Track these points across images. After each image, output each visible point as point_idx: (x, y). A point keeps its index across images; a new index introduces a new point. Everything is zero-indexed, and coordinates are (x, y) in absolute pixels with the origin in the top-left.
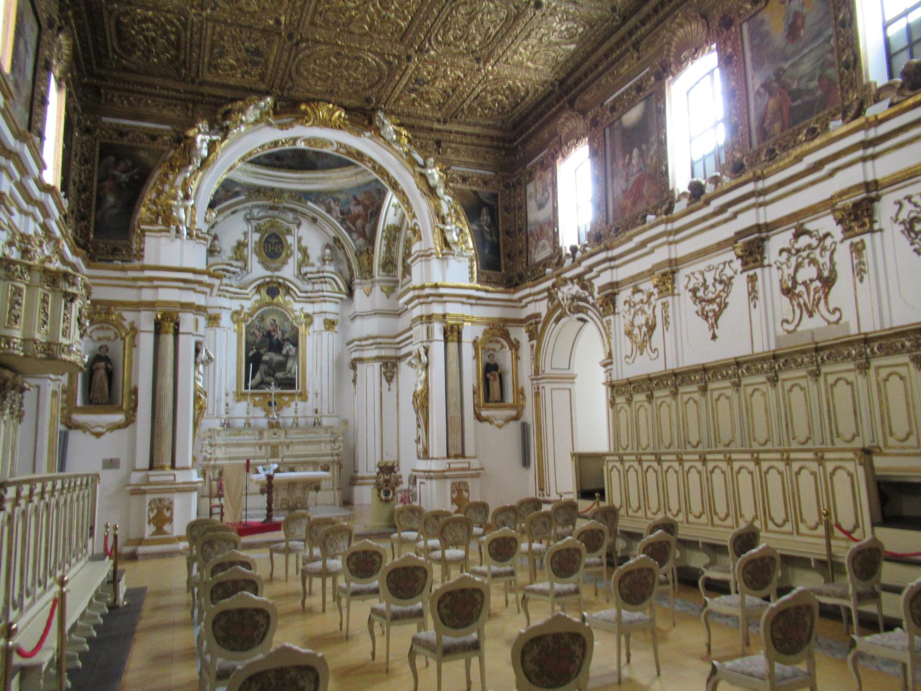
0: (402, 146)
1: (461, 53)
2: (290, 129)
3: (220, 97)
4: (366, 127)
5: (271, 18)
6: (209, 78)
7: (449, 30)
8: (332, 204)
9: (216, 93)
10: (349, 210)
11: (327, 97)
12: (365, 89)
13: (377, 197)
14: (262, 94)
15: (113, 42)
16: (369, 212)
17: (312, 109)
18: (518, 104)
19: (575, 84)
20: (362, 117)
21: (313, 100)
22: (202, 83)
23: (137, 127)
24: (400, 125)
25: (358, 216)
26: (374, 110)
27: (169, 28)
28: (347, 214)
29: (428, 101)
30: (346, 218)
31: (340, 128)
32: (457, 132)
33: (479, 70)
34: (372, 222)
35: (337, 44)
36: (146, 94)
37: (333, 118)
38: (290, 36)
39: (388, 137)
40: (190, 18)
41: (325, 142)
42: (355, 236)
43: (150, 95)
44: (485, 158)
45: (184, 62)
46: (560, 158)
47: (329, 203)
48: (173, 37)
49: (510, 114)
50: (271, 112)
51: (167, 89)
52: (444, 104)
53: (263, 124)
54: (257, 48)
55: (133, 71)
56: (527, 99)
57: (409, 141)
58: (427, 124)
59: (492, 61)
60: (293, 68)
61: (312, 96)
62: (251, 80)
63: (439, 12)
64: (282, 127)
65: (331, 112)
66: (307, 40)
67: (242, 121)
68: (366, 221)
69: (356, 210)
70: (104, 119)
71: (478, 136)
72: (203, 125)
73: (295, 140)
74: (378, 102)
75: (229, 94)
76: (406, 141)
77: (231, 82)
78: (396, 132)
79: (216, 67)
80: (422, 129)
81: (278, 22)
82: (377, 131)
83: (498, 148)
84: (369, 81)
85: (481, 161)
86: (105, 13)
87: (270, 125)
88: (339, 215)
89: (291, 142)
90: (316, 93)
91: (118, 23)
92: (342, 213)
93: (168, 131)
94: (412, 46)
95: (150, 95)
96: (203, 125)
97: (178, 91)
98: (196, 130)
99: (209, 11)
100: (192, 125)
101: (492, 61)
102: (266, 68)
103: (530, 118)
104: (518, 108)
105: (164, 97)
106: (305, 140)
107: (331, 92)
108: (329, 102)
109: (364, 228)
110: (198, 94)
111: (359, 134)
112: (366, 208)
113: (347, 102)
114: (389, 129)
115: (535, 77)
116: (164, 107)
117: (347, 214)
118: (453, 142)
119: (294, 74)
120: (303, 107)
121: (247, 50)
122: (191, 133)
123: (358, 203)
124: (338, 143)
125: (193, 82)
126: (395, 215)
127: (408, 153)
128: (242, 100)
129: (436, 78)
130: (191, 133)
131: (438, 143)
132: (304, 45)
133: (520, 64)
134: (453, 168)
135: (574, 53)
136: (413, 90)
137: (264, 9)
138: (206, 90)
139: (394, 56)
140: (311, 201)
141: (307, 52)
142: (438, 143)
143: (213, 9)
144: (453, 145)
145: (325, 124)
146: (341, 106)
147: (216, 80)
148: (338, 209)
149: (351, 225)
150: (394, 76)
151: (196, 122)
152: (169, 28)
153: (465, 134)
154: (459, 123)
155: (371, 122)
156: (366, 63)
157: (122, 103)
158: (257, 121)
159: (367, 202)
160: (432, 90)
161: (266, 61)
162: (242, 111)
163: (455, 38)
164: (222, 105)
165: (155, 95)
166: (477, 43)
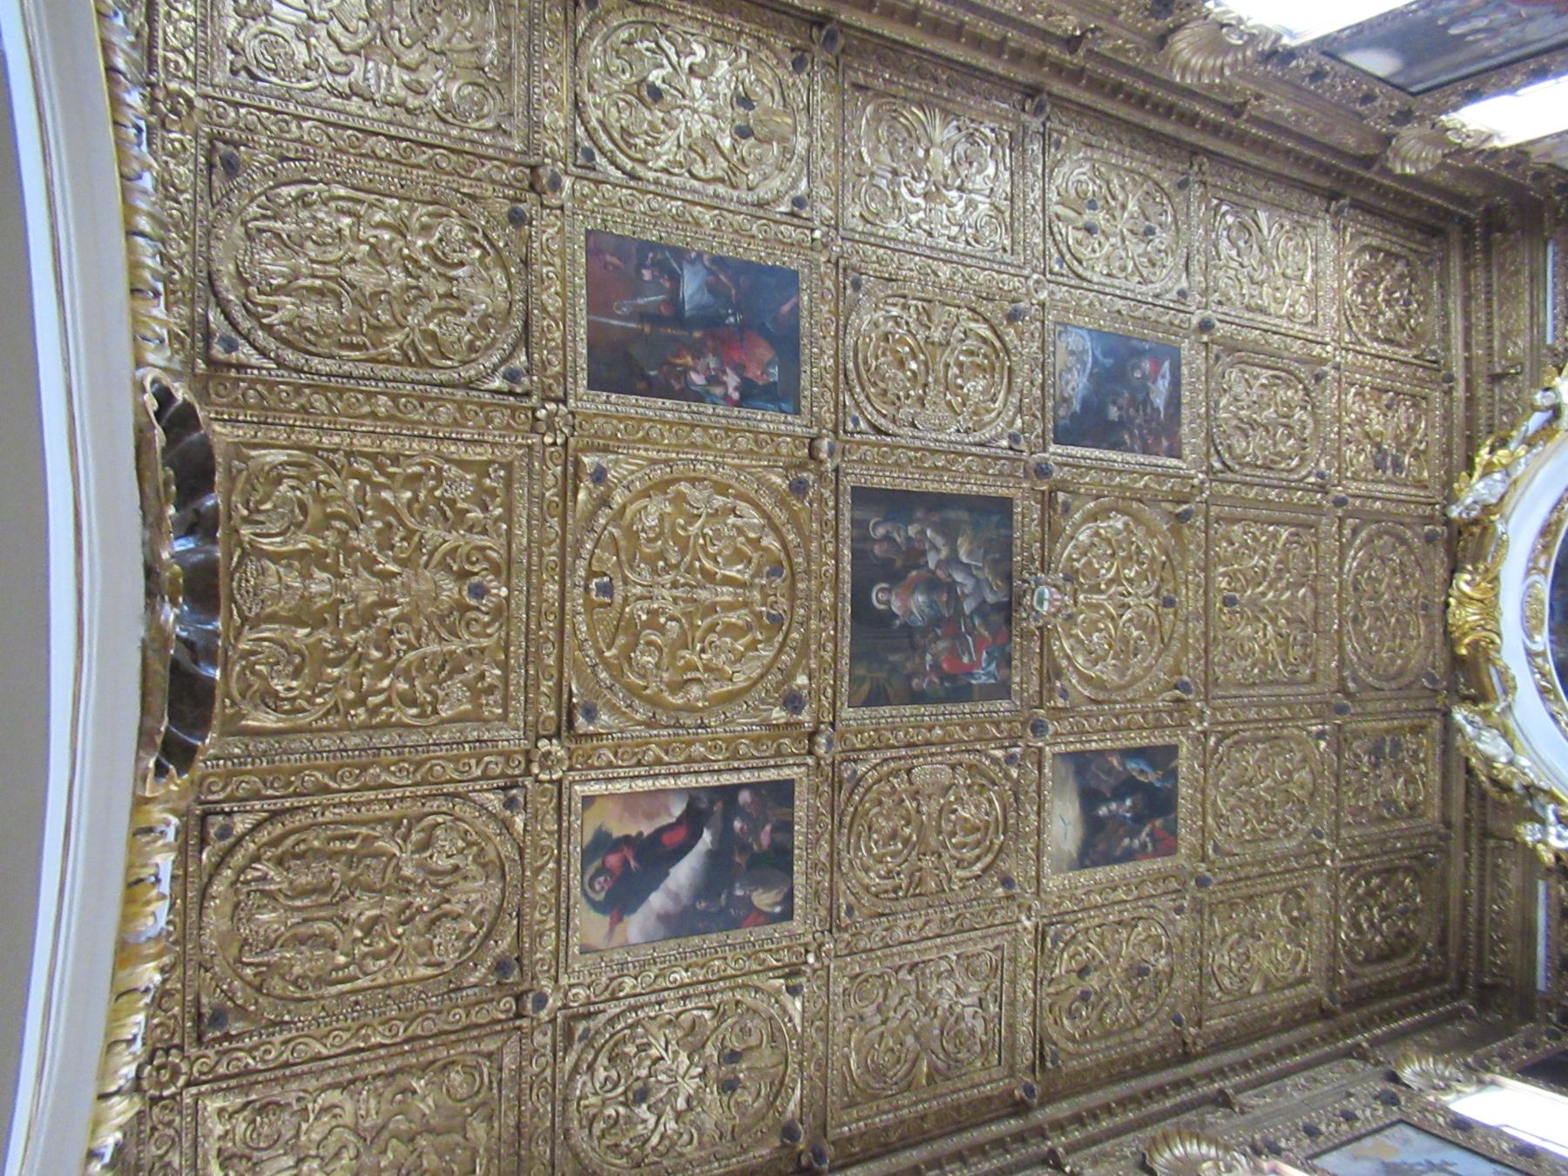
0: (1515, 459)
1: (1313, 414)
2: (1513, 672)
3: (1468, 791)
4: (1485, 529)
5: (1317, 746)
6: (1435, 813)
7: (1279, 454)
9: (1461, 800)
11: (1436, 612)
12: (1410, 550)
14: (1449, 728)
15: (1399, 967)
17: (1465, 635)
18: (1388, 254)
19: (1325, 170)
20: (1466, 542)
21: (1447, 633)
22: (1448, 824)
23: (1548, 937)
24: (1469, 465)
26: (1448, 522)
27: (1360, 891)
29: (1412, 429)
31: (1496, 578)
32: (1467, 346)
33: (1337, 367)
35: (1339, 632)
36: (1481, 910)
37: (1477, 595)
38: (1341, 710)
39: (1500, 489)
40: (1338, 864)
41: (1529, 598)
43: (1481, 904)
44: (1517, 272)
45: (1416, 857)
46: (1497, 143)
48: (1375, 881)
49: (1412, 257)
50: (1482, 706)
51: (1466, 877)
52: (1413, 396)
53: (1511, 723)
54: (1369, 753)
55: (1444, 931)
56: (1375, 242)
57: (1504, 443)
58: (1459, 411)
59: (1317, 350)
60: (1394, 685)
61: (1439, 638)
62: (1427, 745)
63: (1252, 485)
64: (1509, 688)
65: (1464, 600)
66: (1342, 679)
67: (1511, 763)
70: (1541, 984)
71: (1467, 300)
72: (1528, 833)
73: (1531, 655)
74: (1430, 519)
75: (1459, 777)
76: (1501, 452)
77: (1436, 777)
78: (1485, 475)
79: (1412, 807)
80: (1470, 421)
81: (1321, 735)
82: (1487, 509)
83: (1487, 251)
84: (1394, 549)
85: (1524, 279)
86: (1357, 983)
87: (1509, 707)
89: (1539, 660)
90: (1431, 633)
91: (1368, 960)
93: (1548, 888)
94: (1319, 505)
95: (1481, 904)
96: (1528, 833)
97: (1467, 862)
98: (1540, 847)
99: (1324, 842)
100: (1531, 855)
101: (1317, 350)
102: (1402, 727)
103: (1413, 214)
104: (1395, 249)
105: (1481, 883)
106: (1530, 637)
107: (1425, 607)
108: (1447, 605)
110: (1467, 828)
111: (1502, 544)
113: (1441, 572)
114: (1477, 490)
115: (1328, 245)
116: (1503, 886)
118: (1491, 348)
119: (1405, 680)
120: (1464, 651)
121: (1376, 766)
122: (1548, 858)
124: (1528, 573)
125: (1446, 838)
127: (1530, 443)
128: (1467, 760)
129: (1367, 435)
130: (1548, 858)
131: (1495, 378)
132: (1351, 685)
133: (1313, 296)
134: (1549, 341)
135: (1272, 206)
136: (1397, 466)
137: (1304, 760)
138: (1457, 816)
139: (1340, 528)
141: (1362, 672)
142: (1495, 378)
143: (1320, 836)
144: (1496, 344)
145: (1490, 608)
146: (1449, 583)
147: (1436, 801)
150: (1378, 511)
151: (1525, 844)
152: (1360, 891)
153: (1467, 330)
154: (1447, 349)
155: (1476, 522)
156: (1362, 567)
157: (1503, 951)
158: (1505, 734)
160: (1389, 432)
161: (1388, 731)
162: (1488, 761)
163: (1290, 436)
164: (1483, 796)
165: (1481, 897)
166: (1289, 393)
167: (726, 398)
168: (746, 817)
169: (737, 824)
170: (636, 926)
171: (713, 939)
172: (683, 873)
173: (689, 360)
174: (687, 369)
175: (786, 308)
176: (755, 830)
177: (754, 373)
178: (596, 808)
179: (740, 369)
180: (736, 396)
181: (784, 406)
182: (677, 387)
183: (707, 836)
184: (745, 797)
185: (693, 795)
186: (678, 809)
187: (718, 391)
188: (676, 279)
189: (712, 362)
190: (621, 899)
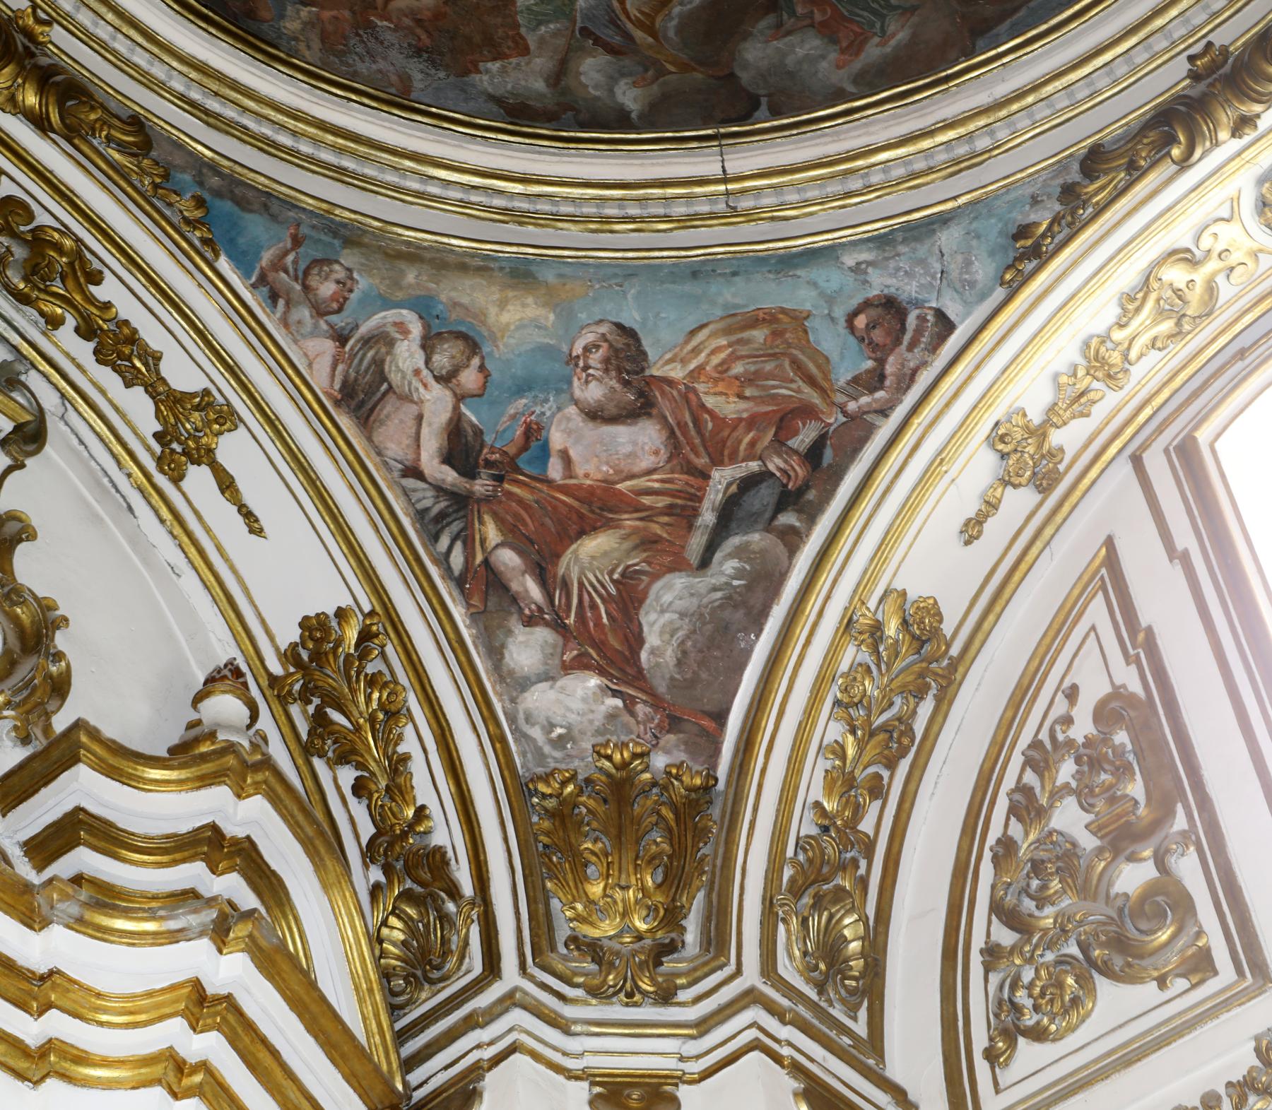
8: (407, 356)
10: (533, 434)
13: (848, 362)
16: (722, 478)
25: (597, 507)
28: (505, 470)
30: (486, 504)
34: (726, 567)
42: (527, 648)
47: (381, 339)
68: (663, 554)
69: (600, 449)
88: (430, 463)
92: (461, 448)
109: (629, 596)
112: (696, 443)
117: (505, 470)
123: (638, 394)
126: (972, 530)
140: (243, 262)
148: (437, 404)
149: (508, 559)
159: (729, 407)
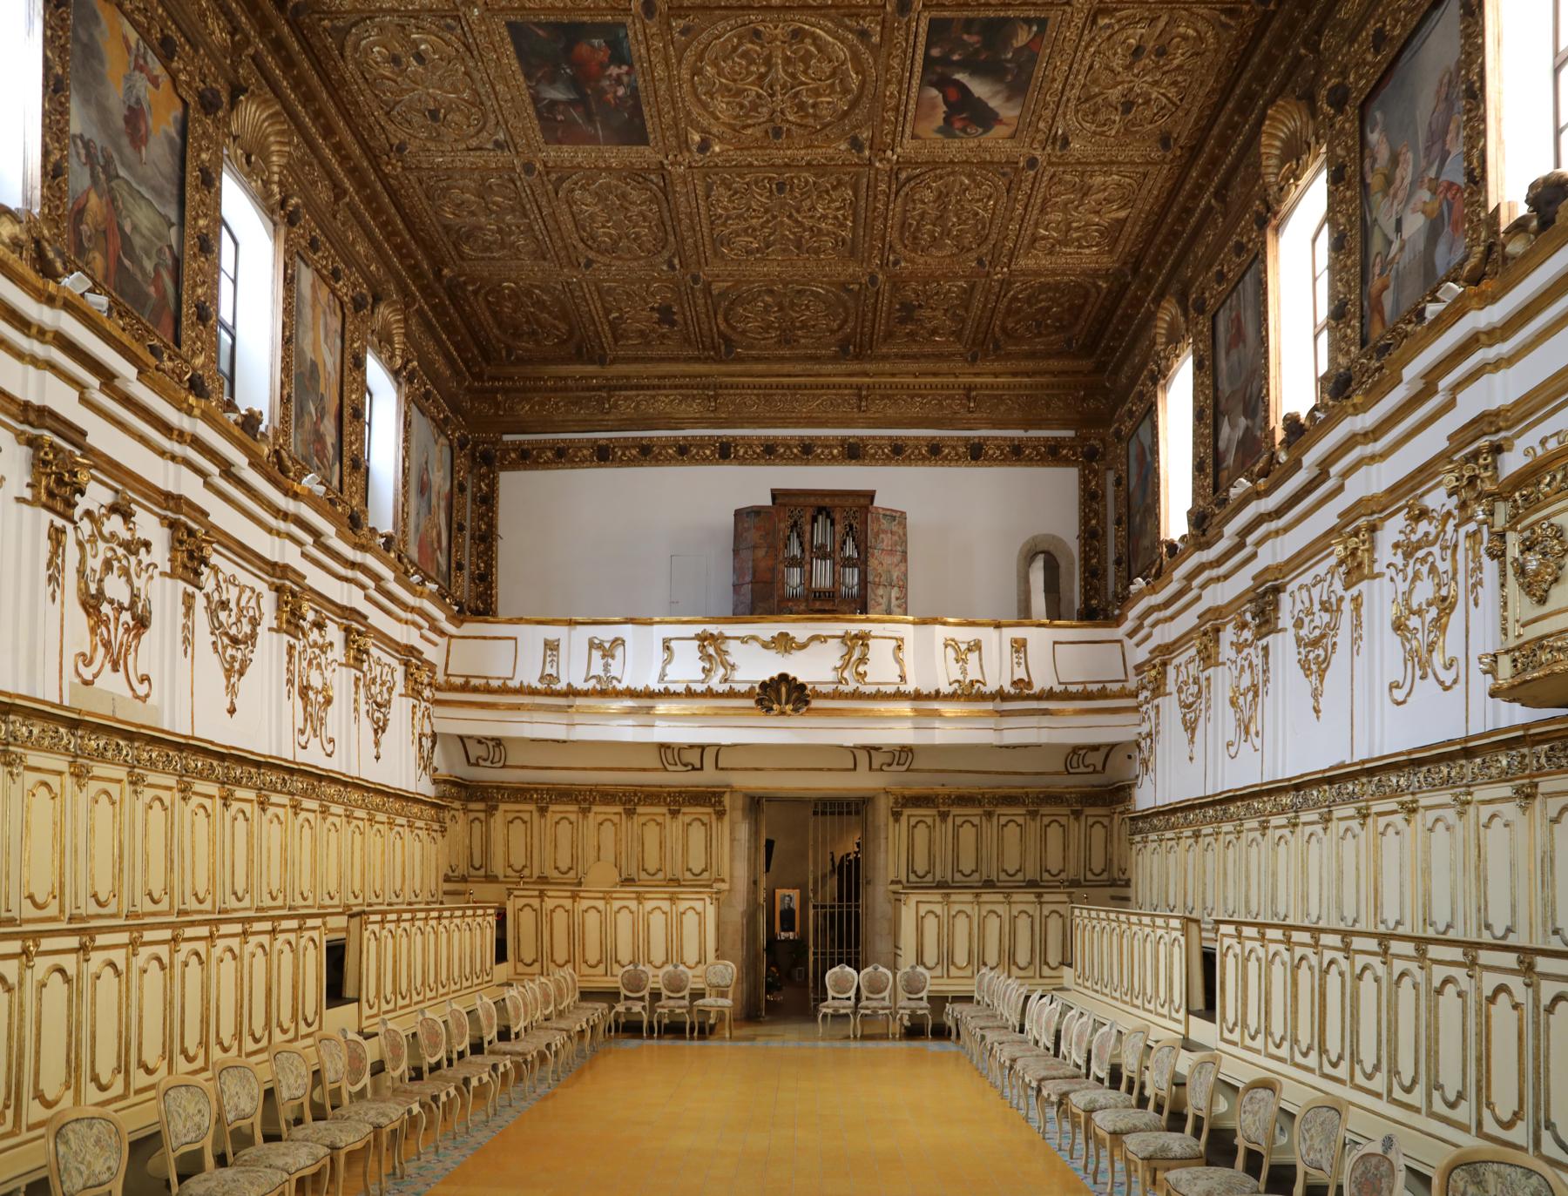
167: (628, 73)
168: (952, 51)
169: (956, 57)
170: (1008, 112)
171: (1039, 73)
172: (980, 89)
173: (609, 96)
174: (616, 97)
175: (540, 32)
176: (964, 45)
177: (603, 55)
178: (918, 132)
179: (604, 67)
180: (625, 68)
181: (621, 35)
182: (631, 102)
183: (959, 76)
184: (935, 52)
185: (926, 82)
186: (934, 92)
187: (625, 79)
188: (554, 103)
189: (606, 83)
190: (984, 118)
